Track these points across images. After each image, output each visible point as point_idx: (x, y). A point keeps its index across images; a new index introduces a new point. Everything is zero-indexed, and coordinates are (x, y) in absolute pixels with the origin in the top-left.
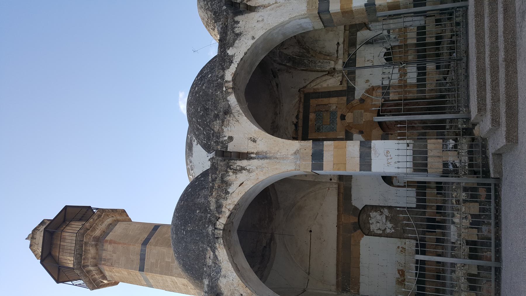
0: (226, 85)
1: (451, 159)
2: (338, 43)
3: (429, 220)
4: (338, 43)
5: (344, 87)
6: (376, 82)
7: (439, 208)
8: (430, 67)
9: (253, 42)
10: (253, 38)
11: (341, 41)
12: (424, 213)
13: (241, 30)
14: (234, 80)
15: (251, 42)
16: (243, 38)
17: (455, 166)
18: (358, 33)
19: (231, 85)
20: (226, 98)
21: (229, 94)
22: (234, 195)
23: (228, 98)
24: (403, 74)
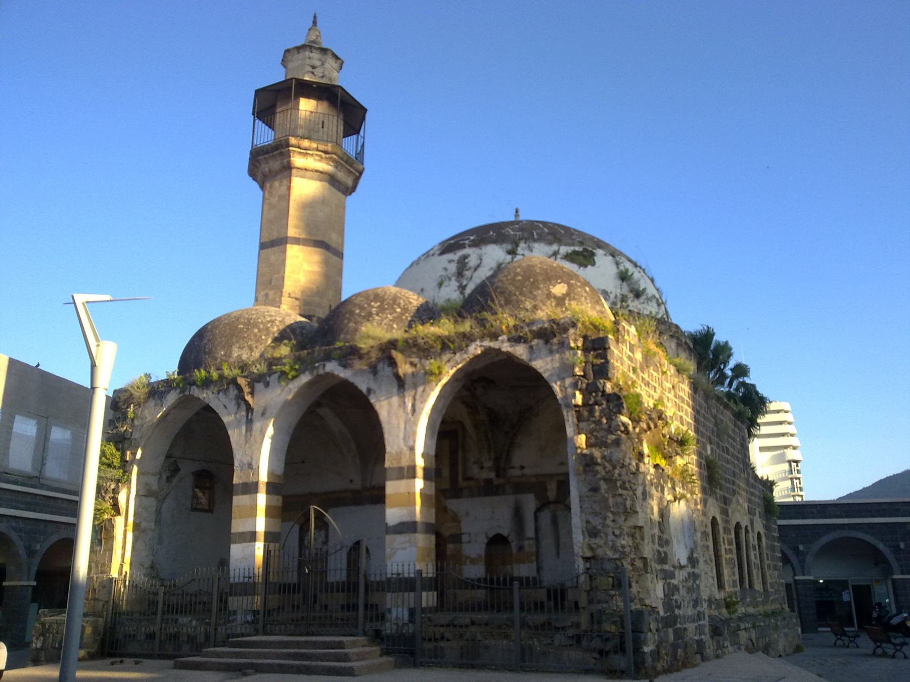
0: (321, 367)
1: (239, 617)
2: (522, 468)
3: (315, 597)
4: (522, 468)
5: (462, 483)
6: (465, 527)
7: (326, 607)
8: (481, 594)
9: (364, 391)
10: (369, 390)
11: (527, 471)
12: (321, 591)
13: (381, 373)
14: (327, 374)
15: (363, 388)
16: (371, 376)
17: (234, 620)
18: (531, 497)
19: (321, 372)
20: (306, 369)
21: (311, 373)
22: (216, 400)
23: (307, 372)
24: (473, 561)
